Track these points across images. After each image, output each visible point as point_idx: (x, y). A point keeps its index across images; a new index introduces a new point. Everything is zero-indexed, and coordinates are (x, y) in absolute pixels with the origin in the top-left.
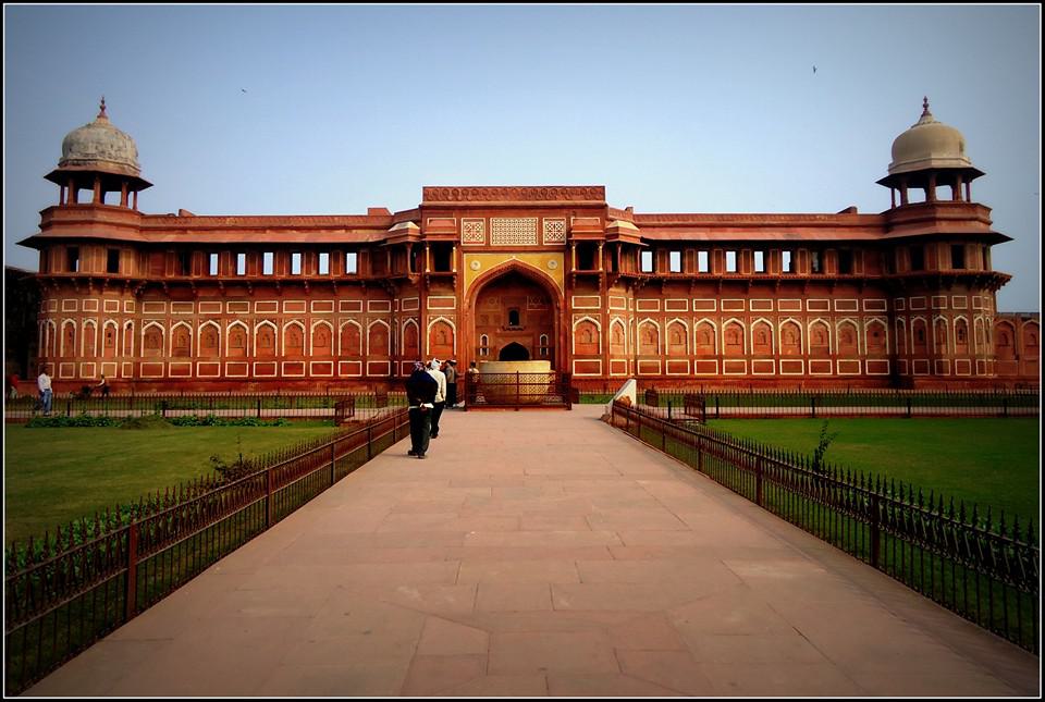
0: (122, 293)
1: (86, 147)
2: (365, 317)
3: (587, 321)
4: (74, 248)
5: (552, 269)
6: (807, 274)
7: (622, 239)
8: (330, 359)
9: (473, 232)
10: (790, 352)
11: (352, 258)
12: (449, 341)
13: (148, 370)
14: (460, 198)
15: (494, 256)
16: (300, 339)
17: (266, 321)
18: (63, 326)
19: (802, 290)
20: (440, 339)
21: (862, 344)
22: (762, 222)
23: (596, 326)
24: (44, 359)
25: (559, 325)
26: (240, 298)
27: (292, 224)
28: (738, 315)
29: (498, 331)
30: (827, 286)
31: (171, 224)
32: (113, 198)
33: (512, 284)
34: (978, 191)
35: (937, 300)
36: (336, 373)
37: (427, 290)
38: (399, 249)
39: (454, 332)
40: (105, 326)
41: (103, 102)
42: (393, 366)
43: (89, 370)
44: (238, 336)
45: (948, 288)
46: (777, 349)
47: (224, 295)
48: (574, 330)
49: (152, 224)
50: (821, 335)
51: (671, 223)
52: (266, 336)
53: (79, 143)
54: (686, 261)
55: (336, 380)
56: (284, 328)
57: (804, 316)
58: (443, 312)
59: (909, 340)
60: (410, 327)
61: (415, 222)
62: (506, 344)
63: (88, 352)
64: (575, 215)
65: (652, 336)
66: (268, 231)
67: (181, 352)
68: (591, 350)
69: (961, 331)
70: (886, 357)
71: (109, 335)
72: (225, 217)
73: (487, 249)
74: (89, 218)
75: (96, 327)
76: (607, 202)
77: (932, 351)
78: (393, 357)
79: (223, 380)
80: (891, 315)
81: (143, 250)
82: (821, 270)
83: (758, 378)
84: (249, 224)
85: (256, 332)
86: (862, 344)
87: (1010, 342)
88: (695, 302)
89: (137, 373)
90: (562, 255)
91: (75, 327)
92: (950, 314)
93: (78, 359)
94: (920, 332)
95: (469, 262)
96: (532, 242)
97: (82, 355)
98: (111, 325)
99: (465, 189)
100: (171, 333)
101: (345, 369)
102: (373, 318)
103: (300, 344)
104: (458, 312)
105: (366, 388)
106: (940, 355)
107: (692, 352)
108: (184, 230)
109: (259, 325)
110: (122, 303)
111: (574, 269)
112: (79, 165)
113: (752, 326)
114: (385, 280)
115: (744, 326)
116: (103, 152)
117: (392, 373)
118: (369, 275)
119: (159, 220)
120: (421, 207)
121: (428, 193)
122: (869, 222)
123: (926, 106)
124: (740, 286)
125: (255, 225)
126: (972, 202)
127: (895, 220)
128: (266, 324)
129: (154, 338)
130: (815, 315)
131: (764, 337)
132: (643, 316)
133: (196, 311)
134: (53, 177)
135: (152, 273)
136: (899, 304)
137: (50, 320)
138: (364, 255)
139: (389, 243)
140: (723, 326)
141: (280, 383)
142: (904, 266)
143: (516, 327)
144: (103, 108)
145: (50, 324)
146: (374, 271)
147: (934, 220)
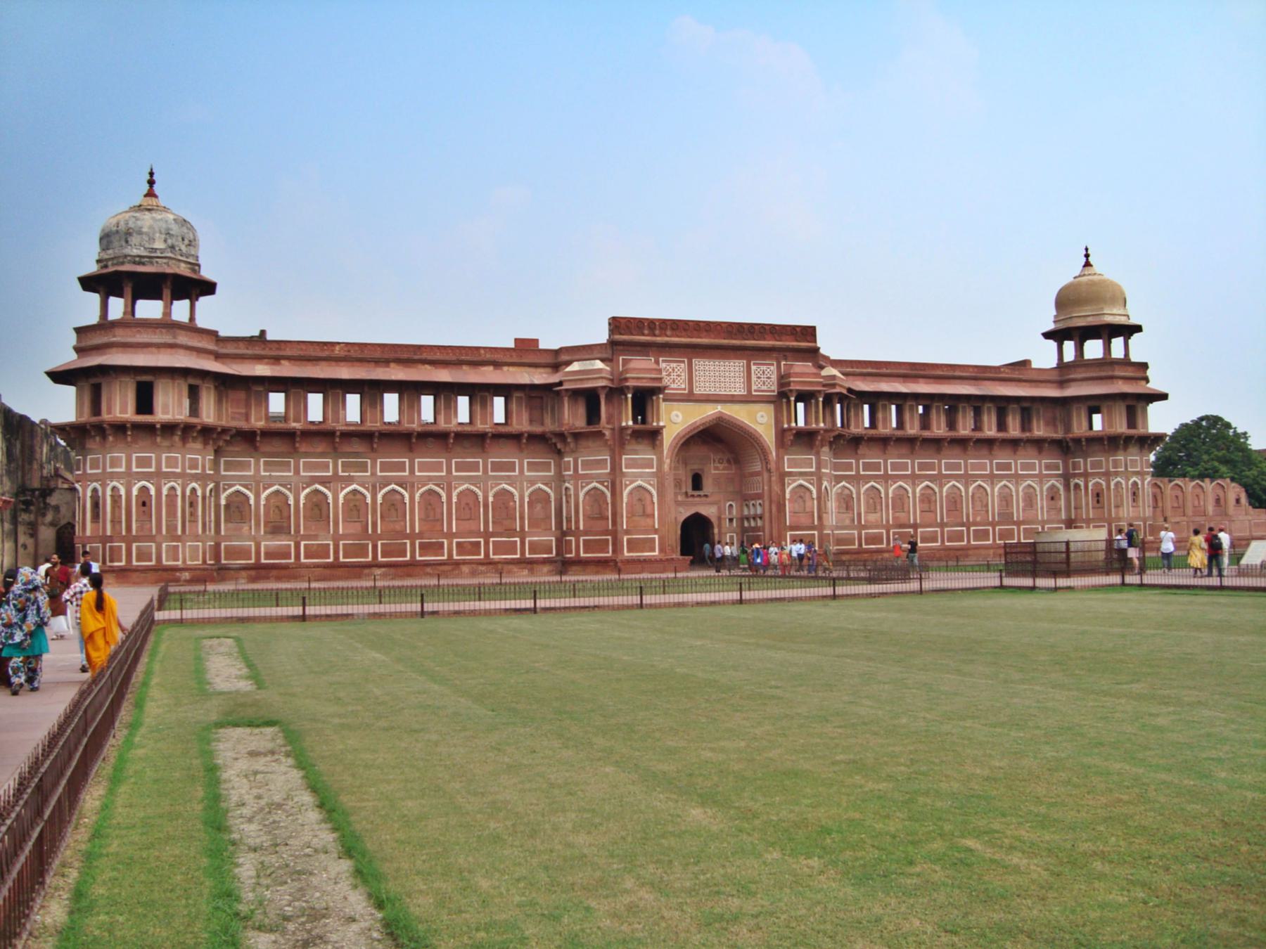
0: (205, 443)
1: (152, 240)
2: (523, 478)
3: (801, 486)
4: (145, 386)
5: (760, 421)
6: (990, 431)
7: (838, 390)
8: (479, 534)
9: (674, 376)
10: (978, 519)
11: (499, 402)
12: (649, 511)
13: (232, 552)
14: (657, 332)
15: (697, 405)
16: (438, 510)
17: (393, 486)
18: (135, 492)
19: (991, 450)
20: (639, 509)
21: (1042, 508)
22: (950, 373)
23: (811, 492)
24: (105, 540)
25: (770, 487)
26: (357, 455)
27: (424, 356)
28: (931, 478)
29: (680, 498)
30: (1014, 444)
31: (257, 351)
32: (180, 310)
33: (717, 439)
34: (1139, 348)
35: (1116, 464)
36: (487, 554)
37: (622, 444)
38: (576, 394)
39: (655, 500)
40: (188, 493)
41: (151, 174)
42: (559, 541)
43: (174, 552)
44: (355, 506)
45: (1125, 449)
46: (968, 515)
47: (335, 449)
48: (788, 496)
49: (230, 349)
50: (1006, 499)
51: (865, 371)
52: (393, 505)
53: (140, 233)
54: (880, 415)
55: (488, 562)
56: (417, 496)
57: (992, 478)
58: (640, 476)
59: (1087, 504)
60: (595, 495)
61: (603, 360)
62: (688, 514)
63: (172, 528)
64: (786, 359)
65: (847, 502)
66: (392, 365)
67: (277, 529)
68: (804, 520)
69: (1134, 494)
70: (1060, 522)
71: (191, 504)
72: (333, 344)
73: (690, 397)
74: (167, 339)
75: (179, 492)
76: (819, 344)
77: (1110, 511)
78: (562, 535)
79: (336, 565)
80: (1066, 478)
81: (225, 383)
82: (978, 427)
83: (950, 549)
84: (367, 354)
85: (379, 500)
86: (1042, 508)
87: (1160, 504)
88: (890, 462)
89: (217, 556)
90: (771, 407)
91: (153, 492)
92: (1127, 475)
93: (158, 539)
94: (1098, 495)
95: (669, 413)
96: (740, 391)
97: (164, 532)
98: (194, 490)
99: (664, 322)
100: (263, 502)
101: (499, 548)
102: (532, 482)
103: (438, 516)
104: (659, 475)
105: (526, 572)
106: (1119, 519)
107: (888, 521)
108: (276, 360)
109: (384, 491)
110: (204, 459)
111: (793, 424)
112: (143, 264)
113: (945, 489)
114: (561, 436)
115: (937, 490)
116: (172, 247)
117: (557, 554)
118: (522, 424)
119: (241, 344)
120: (612, 343)
121: (617, 324)
122: (1041, 378)
123: (1087, 256)
124: (936, 444)
125: (378, 355)
126: (1134, 357)
127: (1072, 376)
128: (394, 490)
129: (237, 509)
130: (1002, 477)
131: (954, 502)
132: (839, 479)
133: (297, 472)
134: (88, 283)
135: (233, 418)
136: (1075, 466)
137: (115, 483)
138: (519, 399)
139: (566, 386)
140: (918, 490)
141: (412, 568)
142: (1079, 429)
143: (701, 493)
144: (151, 183)
145: (114, 488)
146: (531, 421)
147: (1112, 378)
